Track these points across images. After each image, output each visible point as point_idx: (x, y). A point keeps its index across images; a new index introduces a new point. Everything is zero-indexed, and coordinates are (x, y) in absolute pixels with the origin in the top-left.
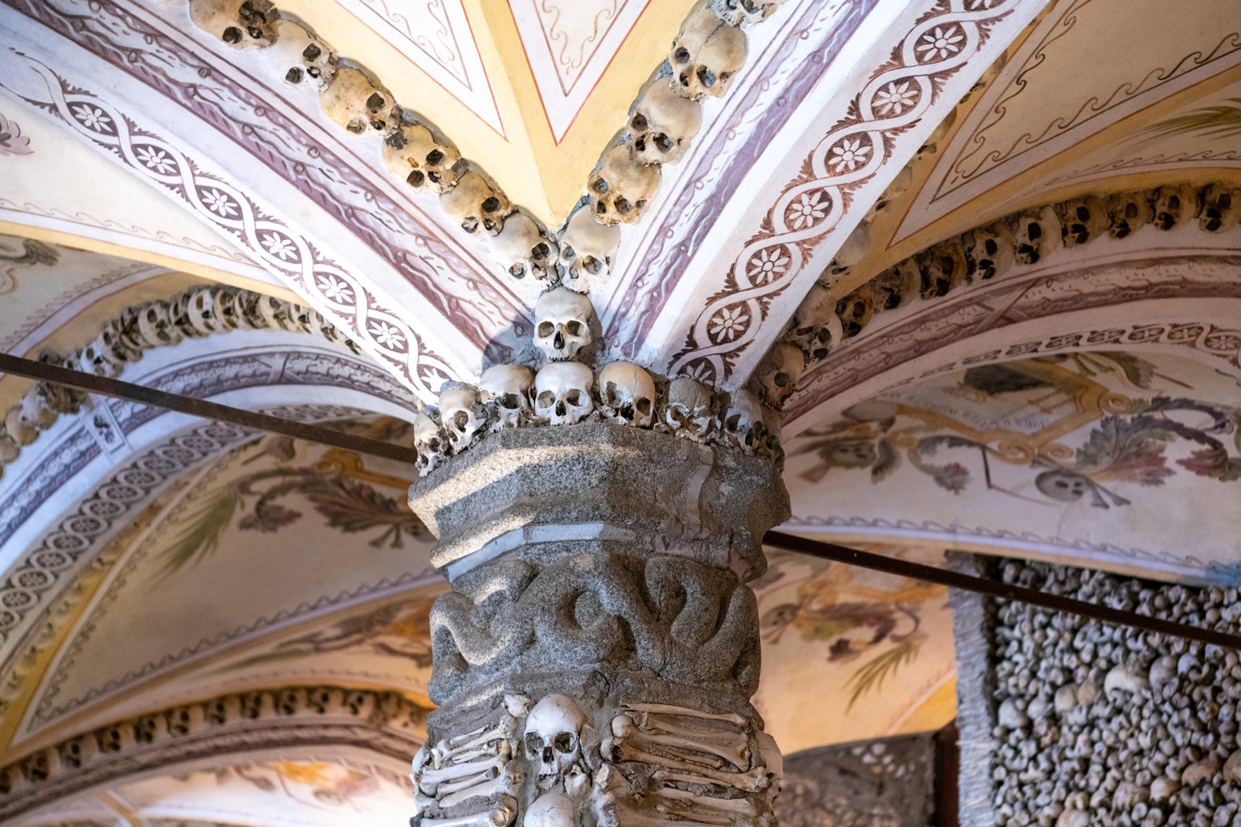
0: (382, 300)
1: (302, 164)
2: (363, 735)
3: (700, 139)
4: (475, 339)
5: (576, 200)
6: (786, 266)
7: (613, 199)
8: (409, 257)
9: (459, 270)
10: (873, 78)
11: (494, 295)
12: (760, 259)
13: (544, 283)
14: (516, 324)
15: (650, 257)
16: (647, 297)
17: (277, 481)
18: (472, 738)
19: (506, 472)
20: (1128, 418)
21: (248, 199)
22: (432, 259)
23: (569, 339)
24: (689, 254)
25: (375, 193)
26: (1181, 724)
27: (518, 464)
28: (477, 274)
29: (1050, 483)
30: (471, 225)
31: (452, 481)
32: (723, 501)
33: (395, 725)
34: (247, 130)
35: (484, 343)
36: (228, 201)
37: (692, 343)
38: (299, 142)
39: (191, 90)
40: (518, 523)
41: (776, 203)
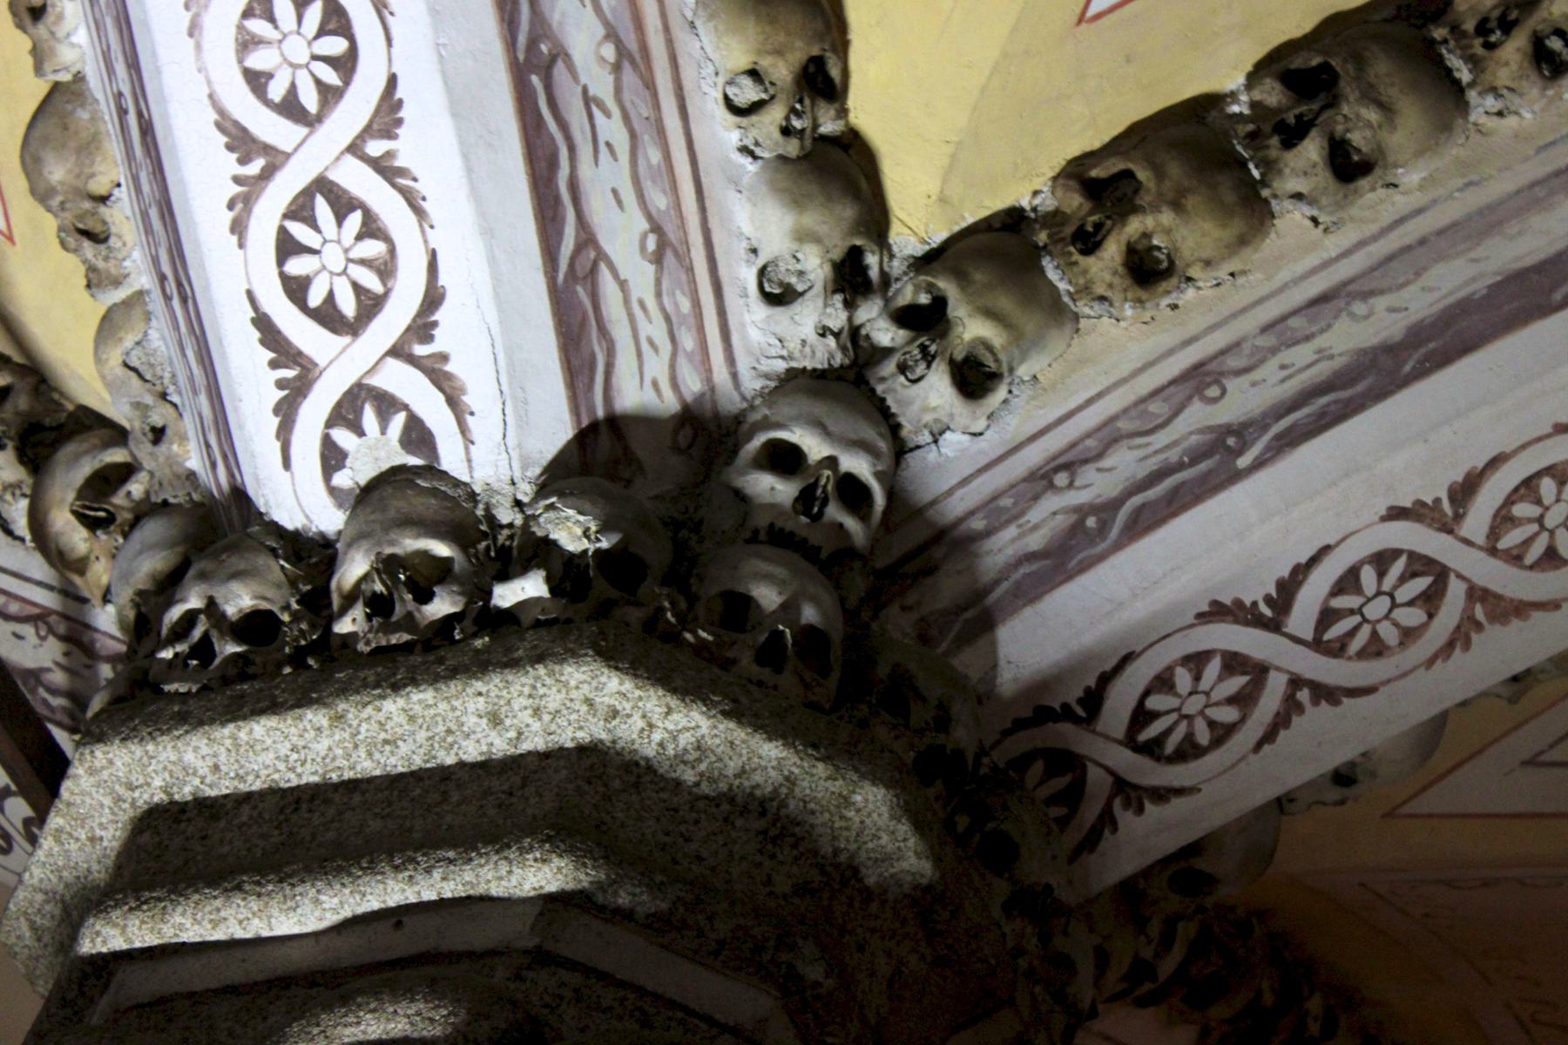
4: (580, 385)
6: (1409, 635)
8: (560, 70)
9: (647, 185)
11: (685, 305)
12: (1381, 575)
13: (825, 354)
15: (1124, 425)
16: (1062, 521)
19: (536, 742)
22: (608, 114)
24: (1243, 462)
27: (594, 730)
30: (748, 93)
31: (316, 717)
35: (592, 409)
37: (1094, 700)
41: (1523, 447)
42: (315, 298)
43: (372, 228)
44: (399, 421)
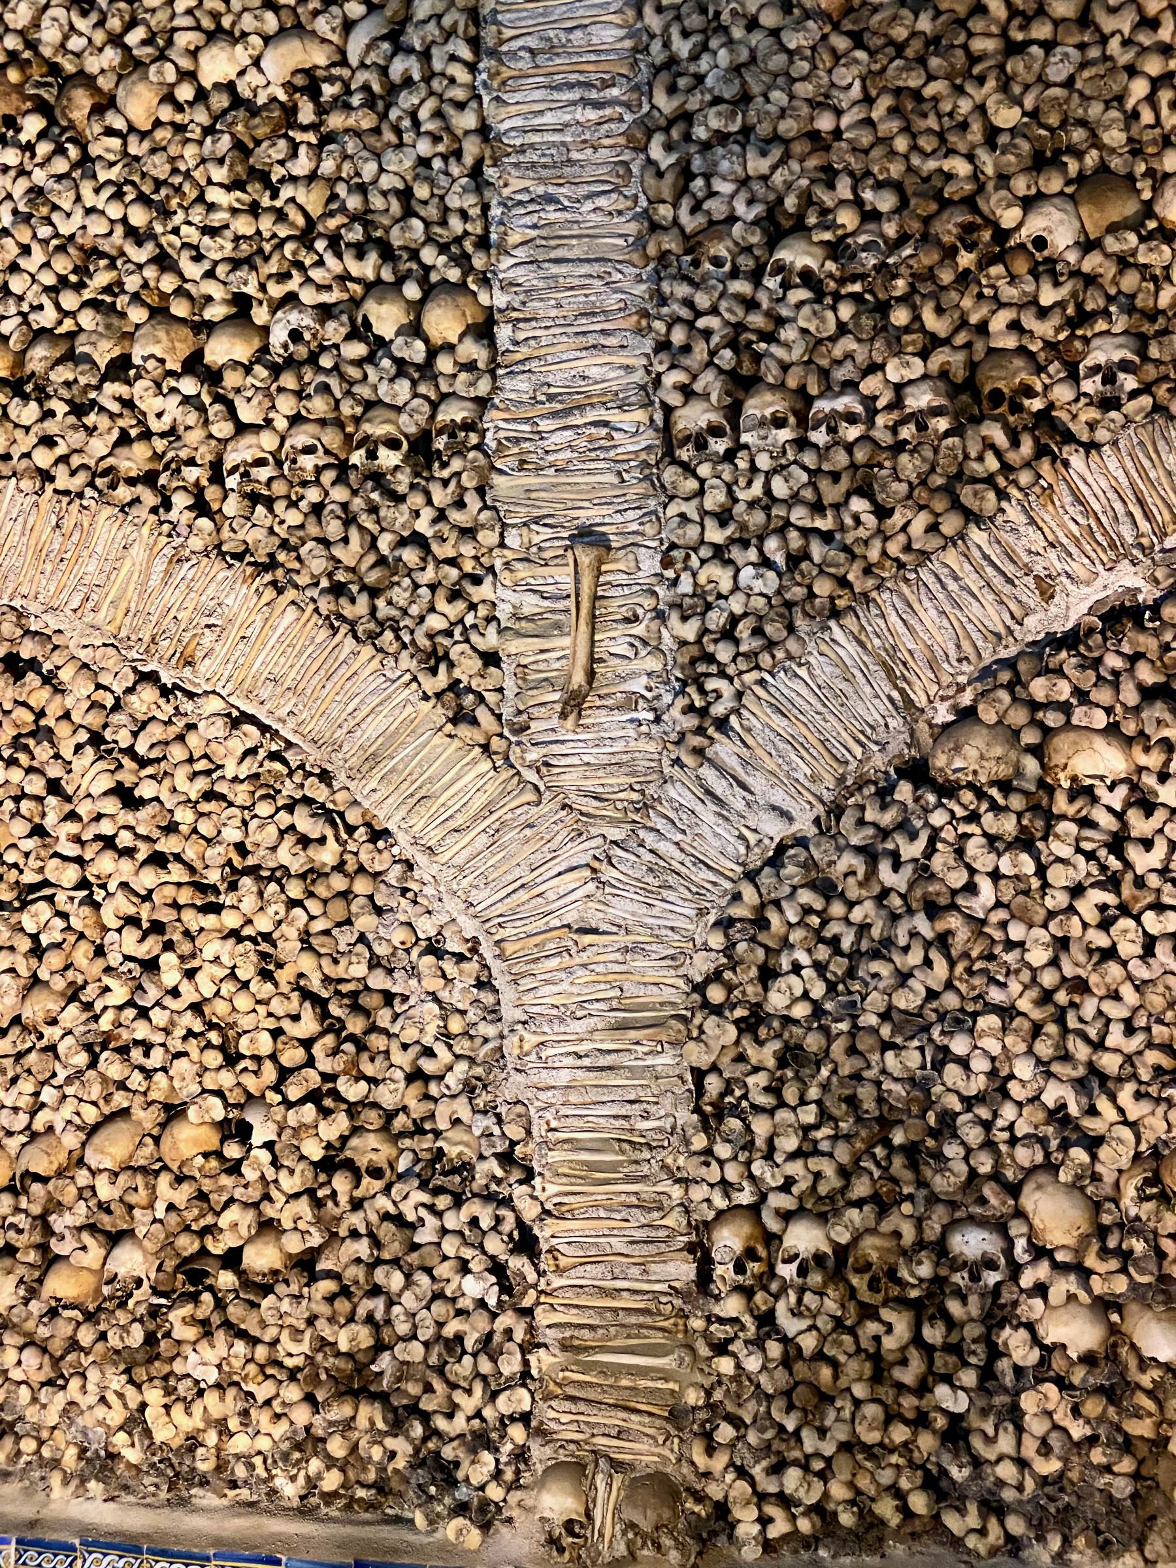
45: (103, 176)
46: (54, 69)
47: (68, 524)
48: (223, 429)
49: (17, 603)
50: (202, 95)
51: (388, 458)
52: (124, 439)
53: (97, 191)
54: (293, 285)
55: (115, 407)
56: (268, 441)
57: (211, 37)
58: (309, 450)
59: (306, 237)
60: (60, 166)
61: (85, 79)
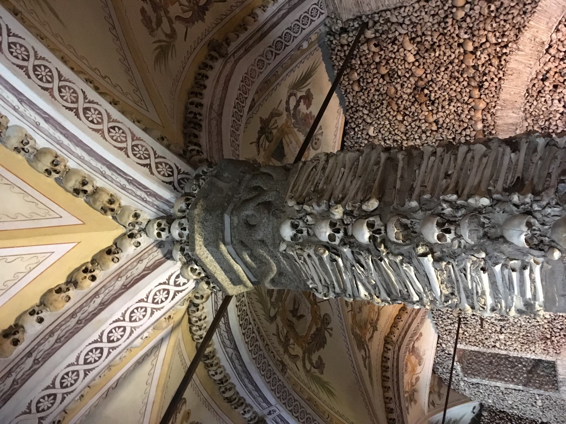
0: (143, 295)
1: (78, 321)
2: (397, 348)
3: (86, 171)
5: (113, 221)
6: (142, 146)
7: (108, 205)
8: (125, 284)
10: (56, 99)
11: (146, 254)
13: (144, 235)
14: (159, 247)
16: (150, 197)
17: (307, 362)
18: (301, 268)
19: (208, 252)
20: (293, 121)
21: (90, 344)
23: (163, 226)
25: (97, 294)
26: (381, 111)
27: (203, 247)
28: (136, 260)
29: (315, 146)
31: (216, 275)
32: (230, 176)
33: (394, 339)
34: (58, 341)
36: (92, 352)
37: (170, 183)
38: (69, 321)
39: (36, 362)
40: (223, 247)
42: (167, 296)
43: (156, 295)
44: (176, 280)
45: (435, 77)
46: (415, 89)
47: (510, 73)
48: (488, 45)
49: (529, 81)
50: (417, 60)
51: (493, 8)
52: (491, 64)
53: (438, 77)
54: (454, 35)
55: (484, 68)
56: (490, 35)
57: (405, 61)
58: (492, 25)
59: (444, 34)
60: (434, 85)
61: (416, 82)
